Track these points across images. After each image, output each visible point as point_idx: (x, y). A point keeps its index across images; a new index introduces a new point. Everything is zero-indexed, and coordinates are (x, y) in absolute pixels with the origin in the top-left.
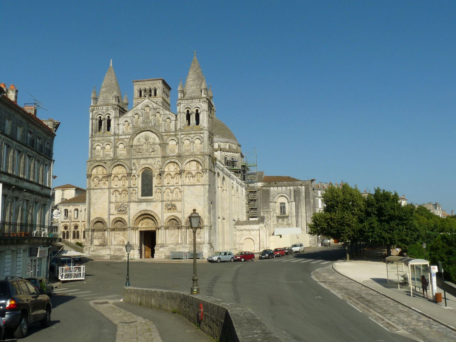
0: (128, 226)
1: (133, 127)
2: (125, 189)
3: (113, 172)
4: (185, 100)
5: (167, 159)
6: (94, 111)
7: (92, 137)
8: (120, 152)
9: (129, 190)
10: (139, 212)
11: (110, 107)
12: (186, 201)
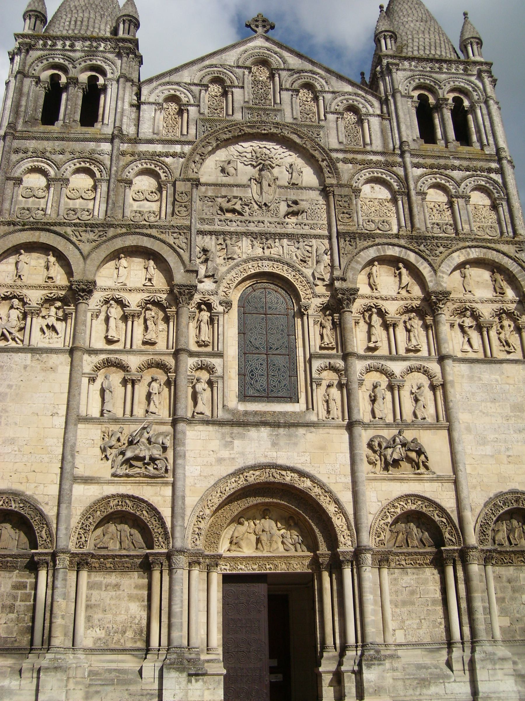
0: (178, 544)
1: (202, 117)
2: (157, 358)
3: (101, 282)
4: (412, 59)
5: (366, 244)
6: (31, 52)
7: (15, 138)
8: (140, 206)
9: (182, 369)
10: (233, 474)
11: (103, 45)
12: (468, 429)
